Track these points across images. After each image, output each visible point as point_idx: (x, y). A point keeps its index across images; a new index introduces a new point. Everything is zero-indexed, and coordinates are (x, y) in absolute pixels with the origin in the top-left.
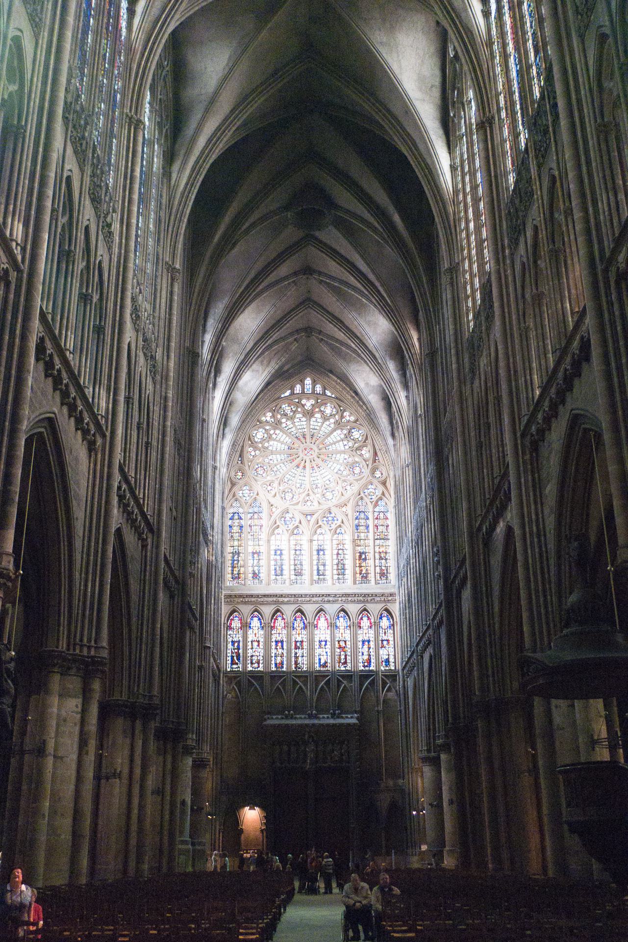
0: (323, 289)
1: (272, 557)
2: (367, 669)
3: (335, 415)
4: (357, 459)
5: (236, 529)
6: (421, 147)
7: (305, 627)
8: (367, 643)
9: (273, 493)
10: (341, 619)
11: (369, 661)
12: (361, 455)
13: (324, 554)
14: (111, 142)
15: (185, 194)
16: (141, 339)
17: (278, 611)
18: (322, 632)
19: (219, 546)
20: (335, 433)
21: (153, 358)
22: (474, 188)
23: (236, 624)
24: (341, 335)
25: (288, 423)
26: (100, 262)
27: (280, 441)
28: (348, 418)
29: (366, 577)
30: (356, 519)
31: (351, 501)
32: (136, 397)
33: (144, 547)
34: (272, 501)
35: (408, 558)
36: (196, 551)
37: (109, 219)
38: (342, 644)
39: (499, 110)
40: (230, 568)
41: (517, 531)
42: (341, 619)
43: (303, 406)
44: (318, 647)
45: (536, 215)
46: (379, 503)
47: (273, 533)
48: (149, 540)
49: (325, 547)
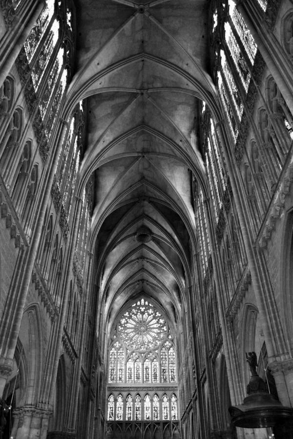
0: (148, 264)
1: (127, 371)
4: (162, 331)
5: (112, 359)
6: (184, 211)
7: (140, 402)
9: (128, 344)
10: (155, 398)
12: (163, 330)
14: (69, 206)
15: (96, 228)
16: (76, 279)
17: (129, 394)
18: (147, 403)
19: (106, 366)
21: (81, 287)
22: (204, 224)
23: (112, 399)
24: (155, 282)
25: (135, 316)
26: (61, 248)
27: (131, 324)
32: (73, 302)
33: (73, 363)
34: (127, 348)
35: (183, 371)
36: (96, 368)
37: (66, 233)
38: (156, 409)
39: (211, 196)
41: (226, 356)
42: (155, 398)
43: (141, 310)
45: (227, 231)
47: (128, 361)
48: (76, 361)
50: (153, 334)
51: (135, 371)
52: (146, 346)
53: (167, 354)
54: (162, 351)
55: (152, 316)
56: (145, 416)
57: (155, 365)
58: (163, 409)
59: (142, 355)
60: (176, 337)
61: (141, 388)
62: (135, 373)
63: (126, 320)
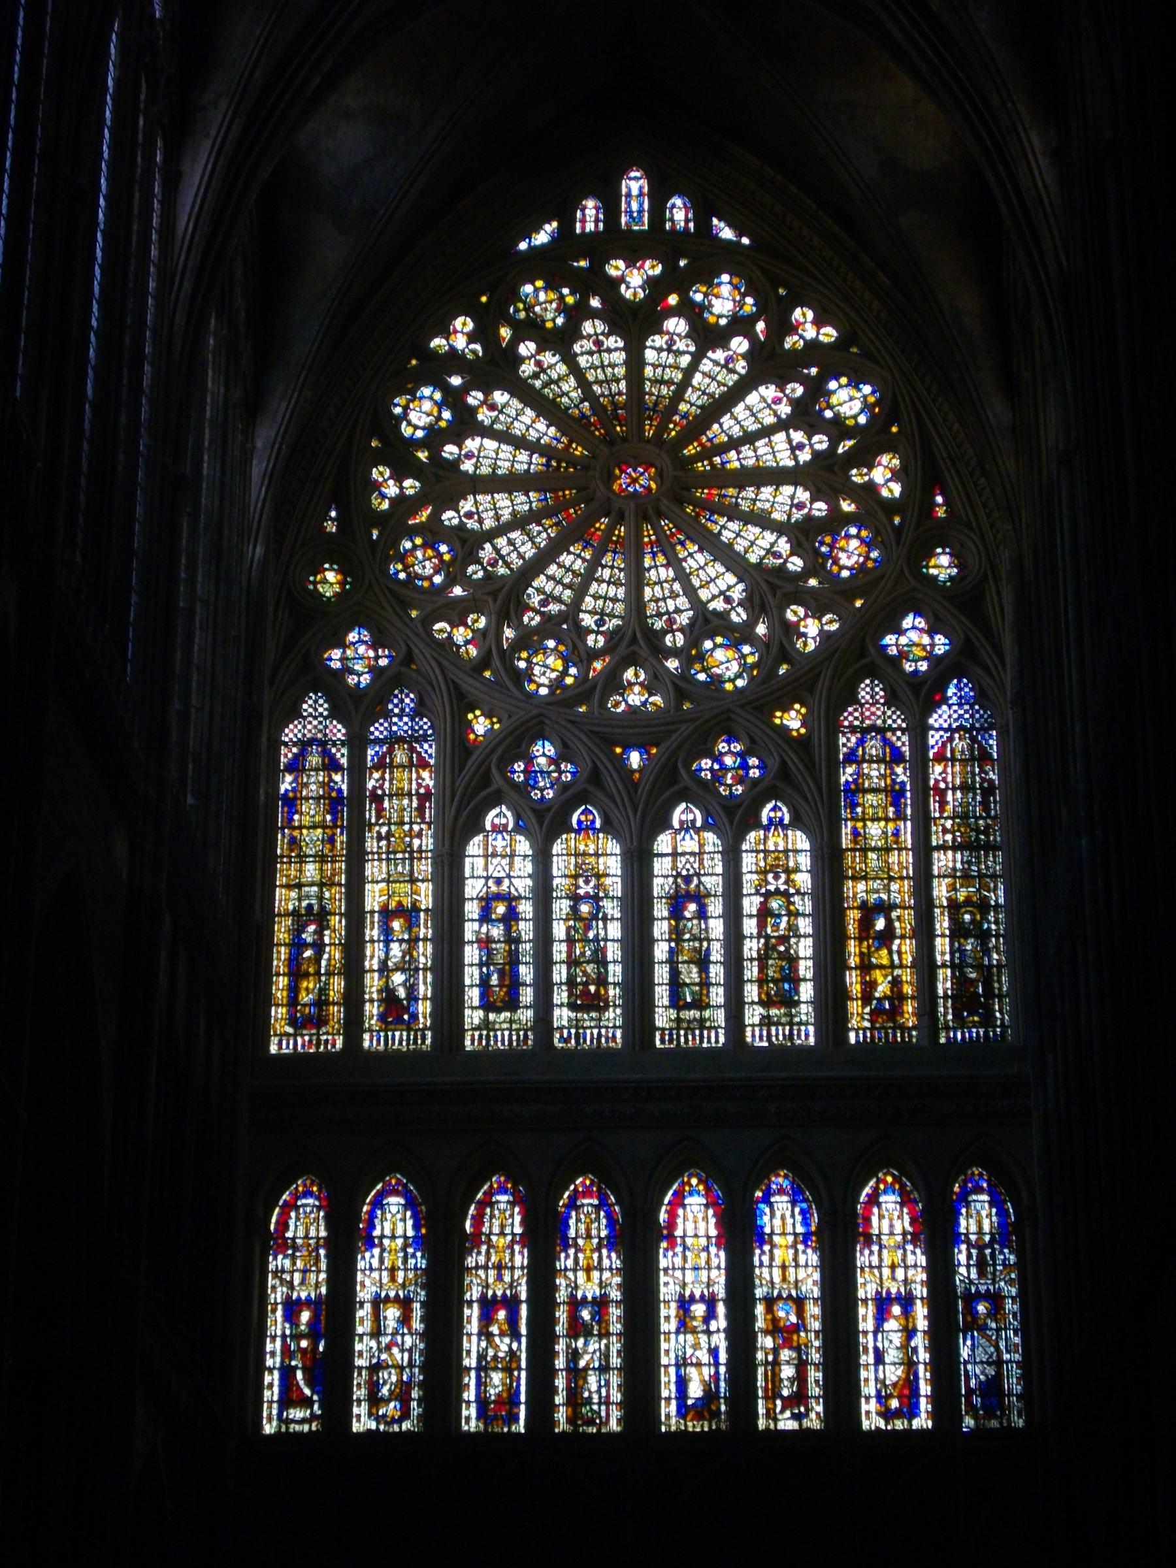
2: (899, 1425)
3: (752, 319)
4: (847, 506)
5: (309, 812)
8: (896, 1310)
10: (781, 1203)
11: (909, 1386)
12: (871, 488)
13: (702, 914)
20: (752, 399)
25: (548, 358)
28: (810, 332)
29: (896, 1011)
38: (786, 1314)
40: (283, 981)
42: (781, 1203)
44: (673, 1325)
46: (951, 691)
47: (475, 826)
51: (559, 930)
52: (672, 664)
53: (903, 742)
54: (850, 717)
55: (740, 344)
56: (668, 1389)
57: (778, 865)
58: (866, 1316)
62: (559, 951)
63: (452, 400)
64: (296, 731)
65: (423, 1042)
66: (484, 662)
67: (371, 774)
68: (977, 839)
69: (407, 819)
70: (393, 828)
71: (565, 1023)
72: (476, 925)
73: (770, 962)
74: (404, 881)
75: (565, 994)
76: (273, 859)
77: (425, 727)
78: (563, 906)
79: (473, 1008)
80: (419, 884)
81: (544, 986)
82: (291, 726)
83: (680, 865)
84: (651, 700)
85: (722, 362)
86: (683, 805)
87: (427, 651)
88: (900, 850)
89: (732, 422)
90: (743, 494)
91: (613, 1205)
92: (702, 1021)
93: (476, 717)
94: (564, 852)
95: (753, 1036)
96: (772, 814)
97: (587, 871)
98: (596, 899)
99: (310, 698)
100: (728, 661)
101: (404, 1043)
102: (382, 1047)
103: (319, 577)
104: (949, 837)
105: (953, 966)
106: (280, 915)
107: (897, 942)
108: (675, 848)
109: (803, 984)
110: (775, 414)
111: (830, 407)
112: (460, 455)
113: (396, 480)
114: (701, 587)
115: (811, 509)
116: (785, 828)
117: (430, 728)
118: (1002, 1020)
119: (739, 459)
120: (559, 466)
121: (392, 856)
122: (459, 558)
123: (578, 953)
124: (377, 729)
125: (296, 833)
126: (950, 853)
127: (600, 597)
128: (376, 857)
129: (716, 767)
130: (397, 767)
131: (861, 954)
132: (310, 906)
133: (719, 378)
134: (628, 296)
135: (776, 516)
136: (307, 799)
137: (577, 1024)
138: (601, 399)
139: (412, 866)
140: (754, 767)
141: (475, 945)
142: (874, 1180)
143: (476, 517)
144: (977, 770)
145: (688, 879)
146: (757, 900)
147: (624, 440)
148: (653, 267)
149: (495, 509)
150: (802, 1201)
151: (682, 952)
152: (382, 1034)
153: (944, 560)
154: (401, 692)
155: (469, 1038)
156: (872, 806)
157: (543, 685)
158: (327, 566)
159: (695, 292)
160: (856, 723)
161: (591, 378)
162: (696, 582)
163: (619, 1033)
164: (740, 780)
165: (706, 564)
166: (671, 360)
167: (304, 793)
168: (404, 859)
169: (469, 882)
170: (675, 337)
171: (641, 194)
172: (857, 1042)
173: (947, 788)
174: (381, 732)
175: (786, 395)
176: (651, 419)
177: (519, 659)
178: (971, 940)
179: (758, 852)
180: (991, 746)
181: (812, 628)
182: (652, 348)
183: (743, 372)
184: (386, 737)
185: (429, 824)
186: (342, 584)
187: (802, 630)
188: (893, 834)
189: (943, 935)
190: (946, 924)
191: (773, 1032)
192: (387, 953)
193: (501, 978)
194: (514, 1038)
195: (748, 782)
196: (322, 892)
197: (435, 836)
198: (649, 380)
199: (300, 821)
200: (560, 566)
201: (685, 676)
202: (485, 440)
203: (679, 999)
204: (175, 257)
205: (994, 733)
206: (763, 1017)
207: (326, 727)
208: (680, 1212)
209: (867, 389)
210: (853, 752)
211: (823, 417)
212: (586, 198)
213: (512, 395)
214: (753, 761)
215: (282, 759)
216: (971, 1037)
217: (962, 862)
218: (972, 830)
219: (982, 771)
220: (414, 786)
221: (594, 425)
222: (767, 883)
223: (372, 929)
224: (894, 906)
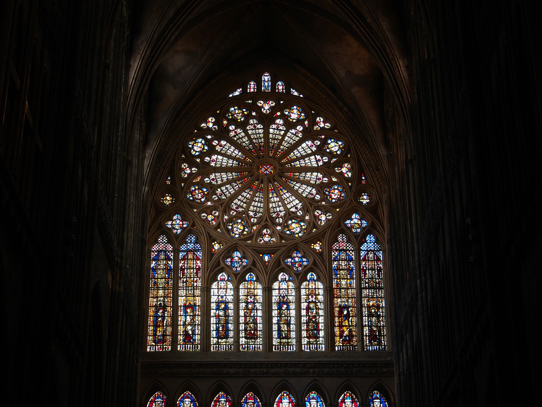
3: (304, 120)
4: (334, 179)
10: (313, 402)
12: (342, 173)
13: (288, 309)
20: (304, 145)
25: (239, 131)
28: (322, 125)
29: (350, 341)
30: (335, 260)
31: (327, 235)
34: (213, 233)
40: (151, 328)
47: (215, 279)
49: (291, 298)
50: (306, 190)
51: (242, 313)
52: (279, 228)
53: (353, 255)
54: (335, 246)
57: (312, 293)
59: (266, 258)
60: (385, 196)
61: (261, 365)
62: (242, 320)
63: (208, 143)
64: (156, 247)
65: (197, 349)
66: (218, 226)
67: (181, 261)
68: (376, 286)
69: (192, 276)
70: (188, 279)
71: (244, 343)
72: (215, 311)
73: (310, 324)
74: (191, 296)
75: (244, 334)
76: (148, 289)
77: (199, 247)
78: (243, 305)
79: (214, 338)
80: (196, 297)
81: (237, 331)
82: (155, 246)
83: (281, 293)
84: (271, 239)
85: (294, 133)
86: (282, 273)
87: (199, 222)
88: (351, 289)
89: (297, 152)
90: (301, 175)
91: (259, 402)
92: (288, 343)
93: (215, 244)
94: (244, 288)
95: (305, 348)
96: (311, 277)
97: (251, 294)
98: (254, 303)
99: (161, 237)
100: (297, 228)
101: (191, 349)
102: (184, 350)
103: (164, 198)
104: (367, 285)
105: (368, 326)
106: (151, 307)
107: (351, 318)
108: (279, 287)
109: (320, 331)
110: (311, 149)
111: (329, 148)
112: (210, 160)
113: (189, 168)
114: (288, 204)
115: (323, 180)
116: (315, 281)
117: (200, 247)
118: (384, 343)
119: (299, 164)
120: (242, 165)
121: (187, 288)
122: (210, 193)
123: (248, 320)
124: (183, 247)
125: (156, 280)
126: (367, 290)
127: (255, 206)
128: (182, 288)
129: (293, 261)
130: (189, 259)
131: (339, 322)
132: (160, 304)
133: (293, 138)
134: (264, 112)
135: (311, 182)
136: (160, 269)
137: (247, 343)
138: (256, 144)
139: (194, 291)
140: (305, 261)
141: (214, 317)
142: (343, 394)
143: (215, 180)
144: (376, 264)
145: (284, 297)
146: (306, 304)
147: (263, 157)
148: (272, 103)
149: (221, 178)
150: (320, 401)
151: (282, 321)
152: (184, 346)
153: (365, 197)
154: (191, 235)
155: (212, 347)
156: (342, 274)
157: (237, 234)
158: (167, 195)
159: (286, 111)
160: (337, 248)
161: (253, 138)
162: (286, 202)
163: (261, 347)
164: (300, 266)
165: (289, 197)
166: (278, 133)
167: (159, 267)
168: (191, 289)
169: (212, 297)
170: (279, 125)
171: (268, 81)
172: (338, 350)
173: (366, 269)
174: (184, 248)
175: (315, 144)
176: (271, 150)
177: (229, 226)
178: (374, 318)
179: (306, 289)
180: (380, 256)
181: (323, 218)
182: (271, 128)
183: (301, 137)
184: (186, 250)
185: (200, 278)
186: (172, 201)
187: (320, 218)
188: (349, 284)
189: (365, 316)
190: (366, 313)
191: (311, 347)
192: (186, 320)
193: (223, 328)
194: (227, 347)
195: (303, 267)
196: (165, 300)
197: (201, 282)
198: (271, 138)
199: (157, 276)
200: (242, 196)
201: (283, 232)
202: (218, 156)
203: (281, 336)
204: (128, 91)
205: (381, 252)
206: (308, 342)
207: (166, 246)
208: (281, 404)
209: (340, 143)
210: (336, 257)
211: (327, 152)
212: (250, 81)
213: (227, 142)
214: (304, 260)
215: (152, 256)
216: (374, 349)
217: (371, 293)
218: (374, 283)
219: (377, 264)
220: (195, 266)
221: (253, 152)
222: (309, 299)
223: (181, 312)
224: (350, 307)
